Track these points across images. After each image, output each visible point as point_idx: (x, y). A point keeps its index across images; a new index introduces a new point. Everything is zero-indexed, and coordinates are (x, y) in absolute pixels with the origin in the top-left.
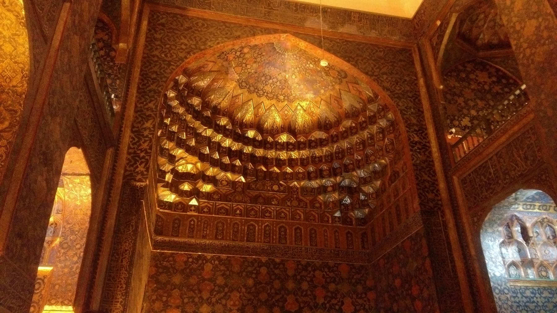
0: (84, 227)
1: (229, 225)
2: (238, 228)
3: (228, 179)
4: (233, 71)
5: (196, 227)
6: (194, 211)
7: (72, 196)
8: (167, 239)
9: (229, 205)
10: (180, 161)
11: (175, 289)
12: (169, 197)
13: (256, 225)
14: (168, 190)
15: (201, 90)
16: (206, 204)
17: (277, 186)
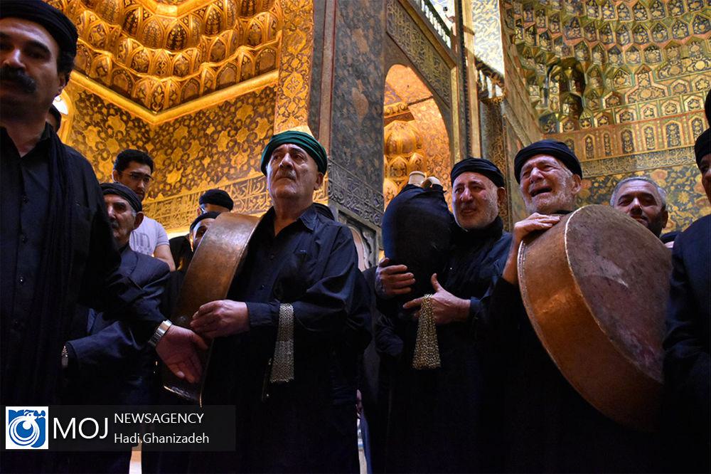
0: (446, 156)
2: (652, 134)
5: (594, 144)
7: (425, 127)
13: (678, 123)
17: (702, 63)
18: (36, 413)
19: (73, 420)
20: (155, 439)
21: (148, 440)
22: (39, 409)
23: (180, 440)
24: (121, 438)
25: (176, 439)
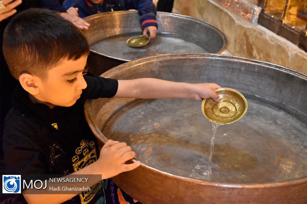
18: (15, 178)
19: (32, 181)
20: (67, 189)
21: (64, 189)
22: (17, 176)
23: (78, 190)
24: (52, 189)
25: (76, 189)
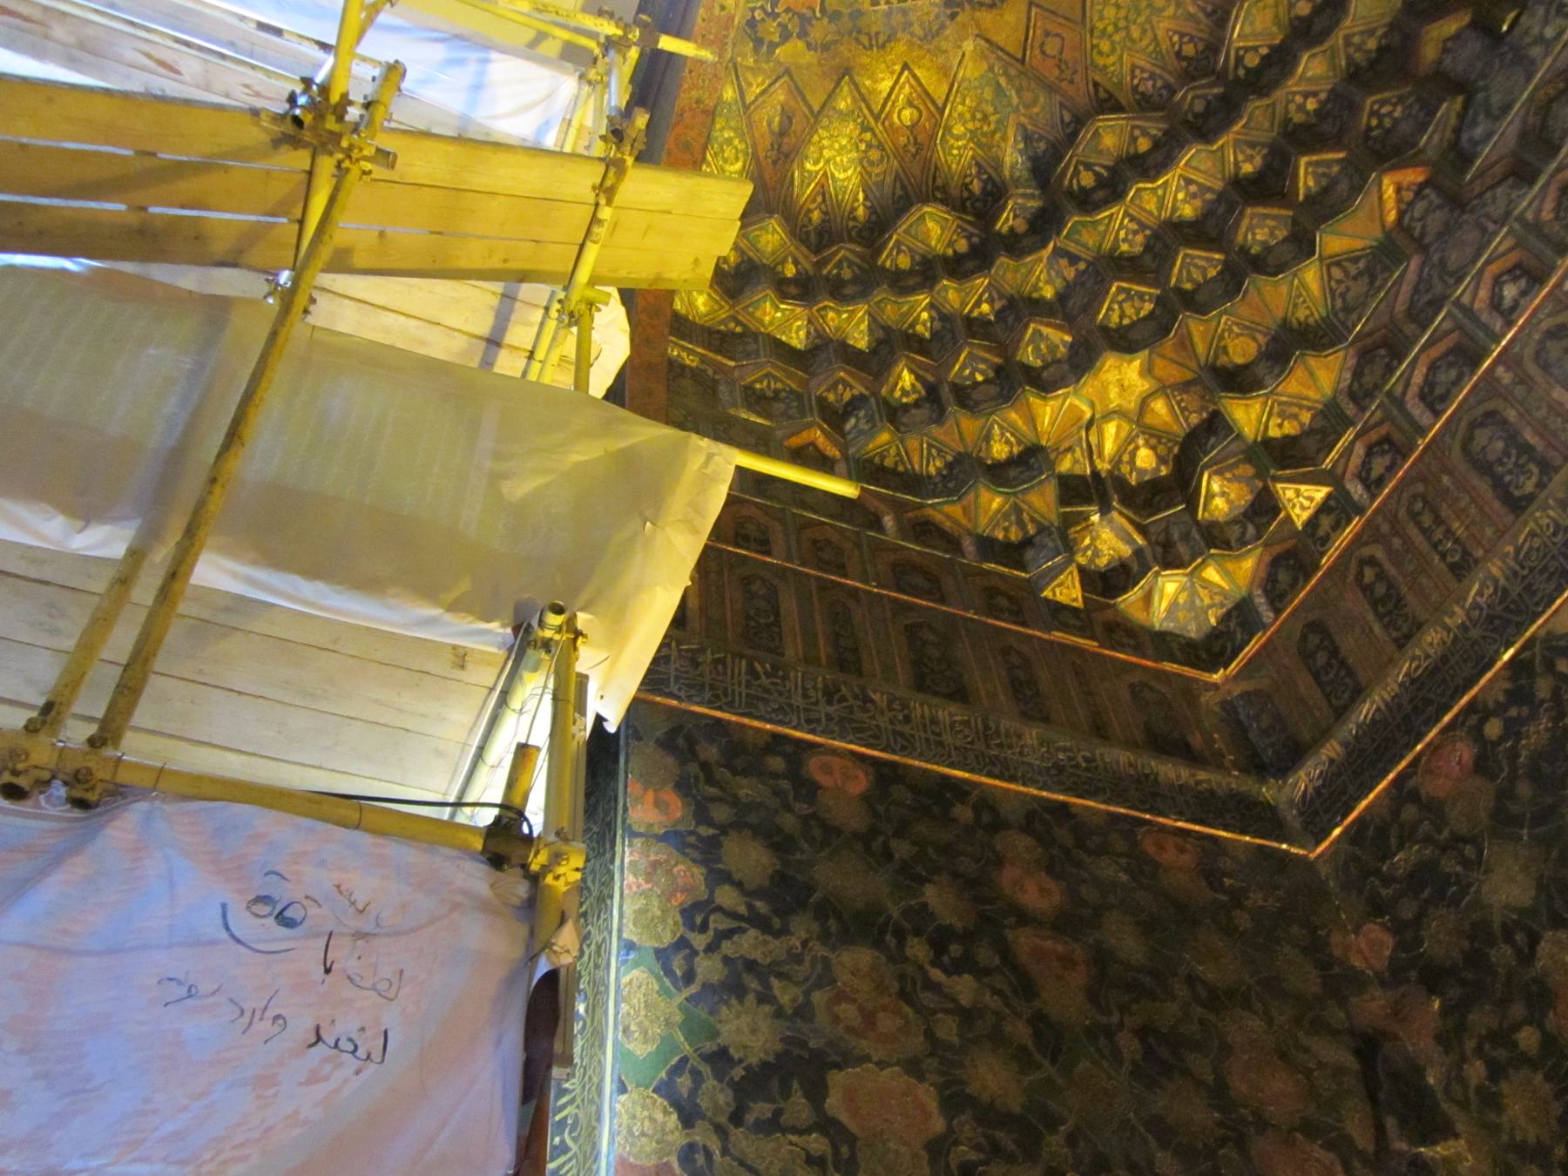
1: (1520, 391)
3: (1355, 260)
4: (888, 14)
5: (1392, 571)
6: (1338, 526)
8: (1331, 750)
9: (1447, 325)
10: (1093, 440)
11: (1534, 940)
12: (1202, 592)
14: (1157, 574)
15: (899, 192)
16: (1359, 450)
